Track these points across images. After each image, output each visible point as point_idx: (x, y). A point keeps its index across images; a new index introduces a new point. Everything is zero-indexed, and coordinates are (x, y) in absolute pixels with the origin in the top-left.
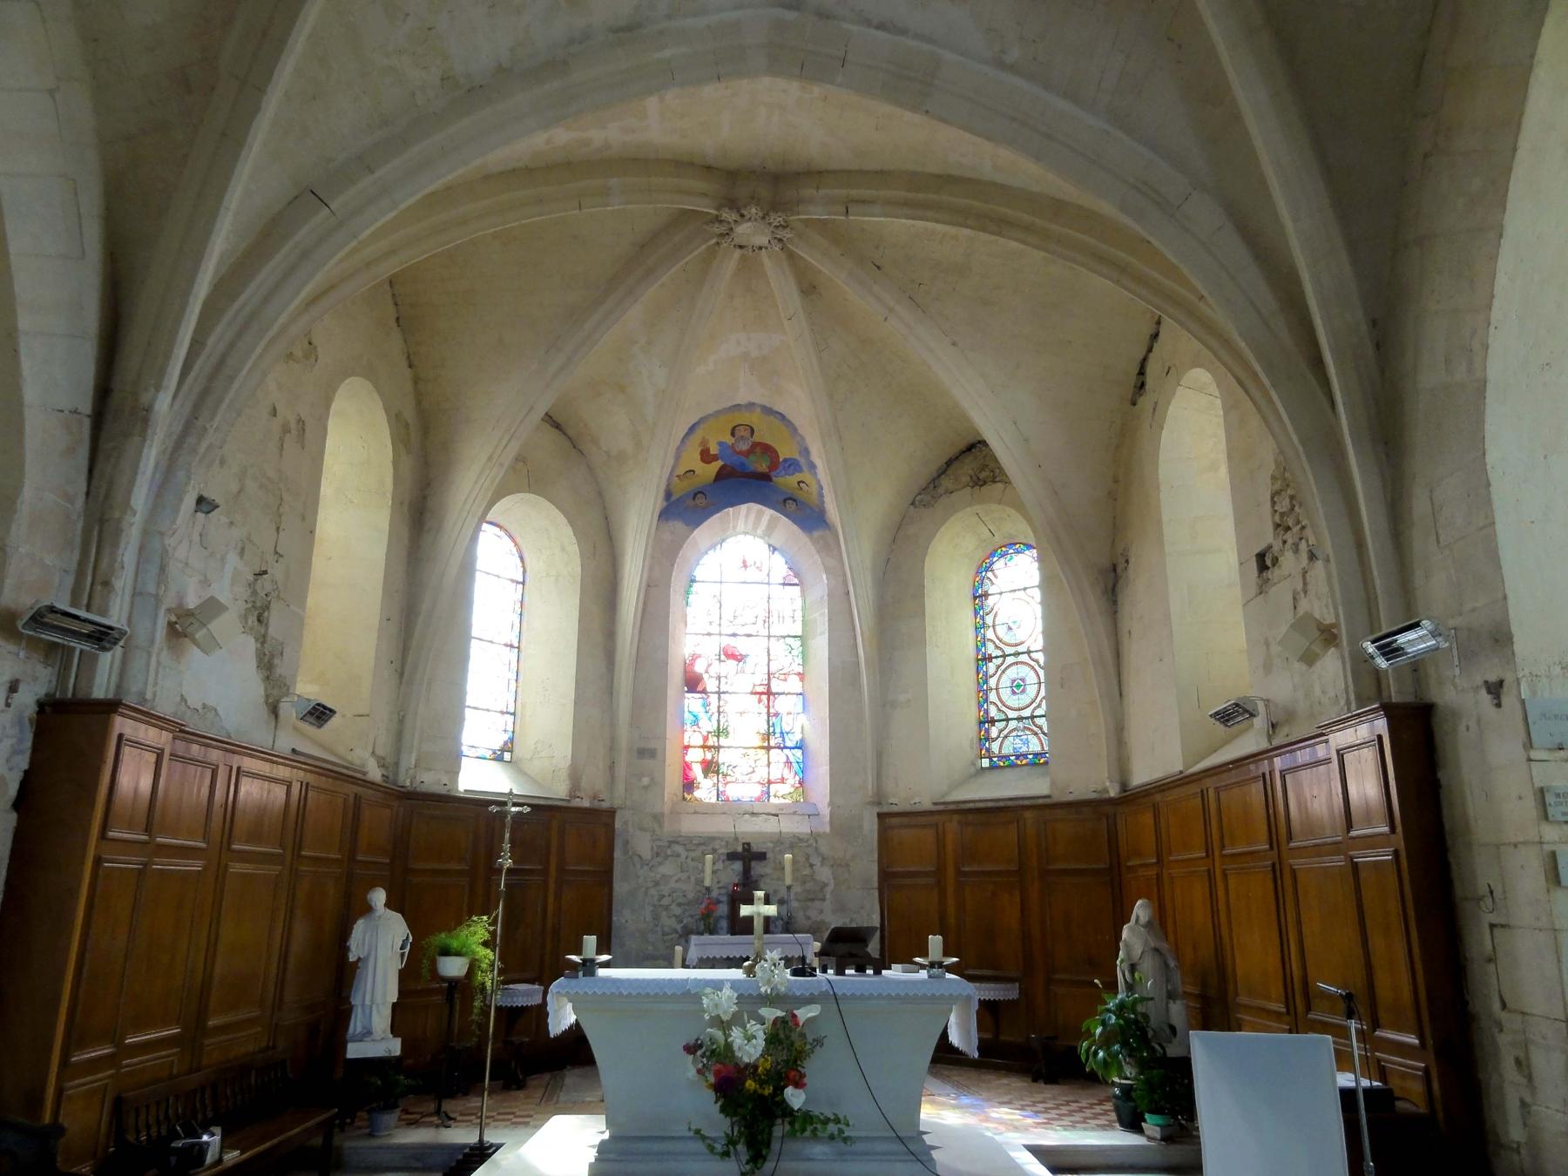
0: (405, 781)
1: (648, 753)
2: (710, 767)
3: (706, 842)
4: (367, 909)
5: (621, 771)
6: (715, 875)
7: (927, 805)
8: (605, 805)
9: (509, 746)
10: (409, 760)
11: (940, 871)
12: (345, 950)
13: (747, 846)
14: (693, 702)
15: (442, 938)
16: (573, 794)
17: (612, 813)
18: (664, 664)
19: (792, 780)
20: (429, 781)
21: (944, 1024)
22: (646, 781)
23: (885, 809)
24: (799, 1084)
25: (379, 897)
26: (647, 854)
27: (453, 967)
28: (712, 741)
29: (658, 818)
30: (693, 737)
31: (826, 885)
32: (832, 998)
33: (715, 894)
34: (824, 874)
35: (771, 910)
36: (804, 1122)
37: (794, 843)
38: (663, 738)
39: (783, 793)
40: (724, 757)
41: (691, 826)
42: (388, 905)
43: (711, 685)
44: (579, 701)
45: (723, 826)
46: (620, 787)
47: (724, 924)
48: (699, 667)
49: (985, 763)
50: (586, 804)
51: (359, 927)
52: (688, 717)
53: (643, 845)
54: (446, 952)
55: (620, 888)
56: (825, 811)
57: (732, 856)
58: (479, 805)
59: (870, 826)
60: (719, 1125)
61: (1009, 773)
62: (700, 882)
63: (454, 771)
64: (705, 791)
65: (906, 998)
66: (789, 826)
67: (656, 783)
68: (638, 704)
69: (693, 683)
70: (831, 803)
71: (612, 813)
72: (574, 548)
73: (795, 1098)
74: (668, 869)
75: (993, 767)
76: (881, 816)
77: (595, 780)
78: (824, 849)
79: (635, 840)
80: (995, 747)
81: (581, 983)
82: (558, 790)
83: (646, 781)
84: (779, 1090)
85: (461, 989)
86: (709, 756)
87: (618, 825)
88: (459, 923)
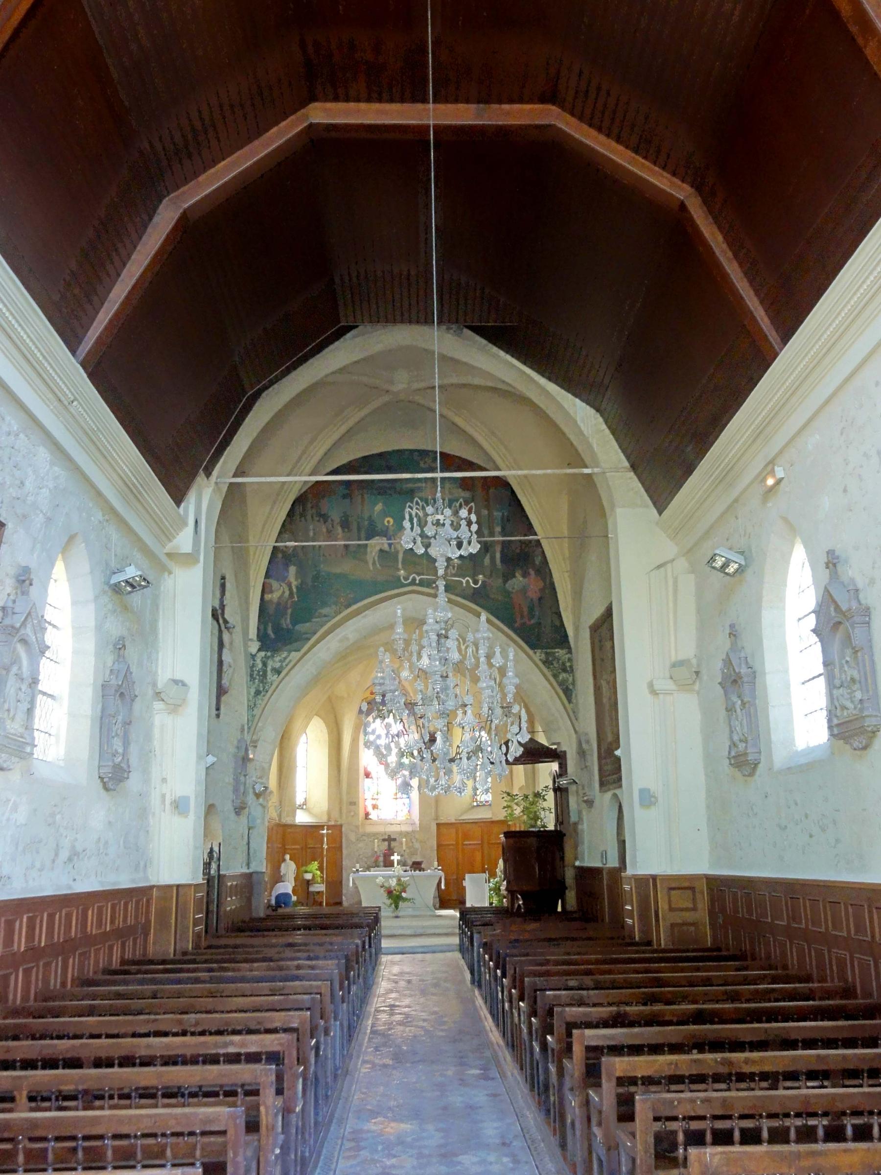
0: (284, 821)
1: (354, 803)
2: (375, 807)
3: (375, 835)
4: (284, 860)
5: (344, 811)
6: (380, 847)
7: (453, 821)
8: (339, 823)
9: (305, 803)
10: (283, 815)
11: (457, 844)
12: (280, 872)
13: (389, 836)
14: (367, 780)
15: (304, 868)
16: (329, 820)
17: (341, 826)
18: (358, 770)
19: (406, 811)
20: (286, 820)
21: (437, 881)
22: (352, 814)
23: (439, 822)
24: (405, 892)
25: (287, 857)
26: (354, 840)
27: (308, 876)
28: (375, 797)
29: (357, 827)
30: (368, 795)
31: (417, 849)
32: (412, 876)
33: (378, 853)
34: (417, 845)
35: (399, 858)
36: (405, 900)
37: (406, 834)
38: (358, 798)
39: (402, 816)
40: (378, 803)
41: (370, 829)
42: (291, 859)
43: (373, 774)
44: (329, 787)
45: (380, 829)
46: (344, 817)
47: (382, 864)
48: (369, 769)
49: (475, 804)
50: (332, 823)
51: (283, 865)
52: (366, 788)
53: (353, 837)
54: (306, 872)
55: (345, 852)
56: (418, 822)
57: (384, 840)
58: (312, 830)
59: (434, 828)
60: (389, 902)
61: (483, 808)
62: (373, 849)
63: (294, 816)
64: (373, 816)
65: (429, 876)
66: (405, 828)
67: (356, 814)
68: (350, 785)
69: (367, 775)
70: (420, 820)
71: (341, 826)
72: (325, 731)
73: (404, 895)
74: (361, 845)
75: (478, 806)
76: (438, 825)
77: (335, 814)
78: (417, 836)
79: (349, 836)
80: (478, 798)
81: (356, 875)
82: (324, 819)
83: (352, 814)
84: (401, 893)
85: (308, 883)
86: (374, 802)
87: (343, 829)
88: (310, 863)
